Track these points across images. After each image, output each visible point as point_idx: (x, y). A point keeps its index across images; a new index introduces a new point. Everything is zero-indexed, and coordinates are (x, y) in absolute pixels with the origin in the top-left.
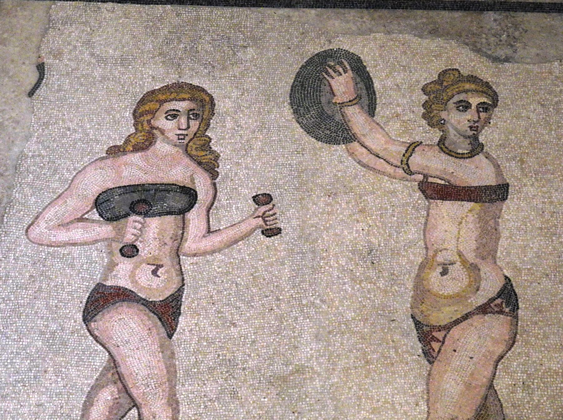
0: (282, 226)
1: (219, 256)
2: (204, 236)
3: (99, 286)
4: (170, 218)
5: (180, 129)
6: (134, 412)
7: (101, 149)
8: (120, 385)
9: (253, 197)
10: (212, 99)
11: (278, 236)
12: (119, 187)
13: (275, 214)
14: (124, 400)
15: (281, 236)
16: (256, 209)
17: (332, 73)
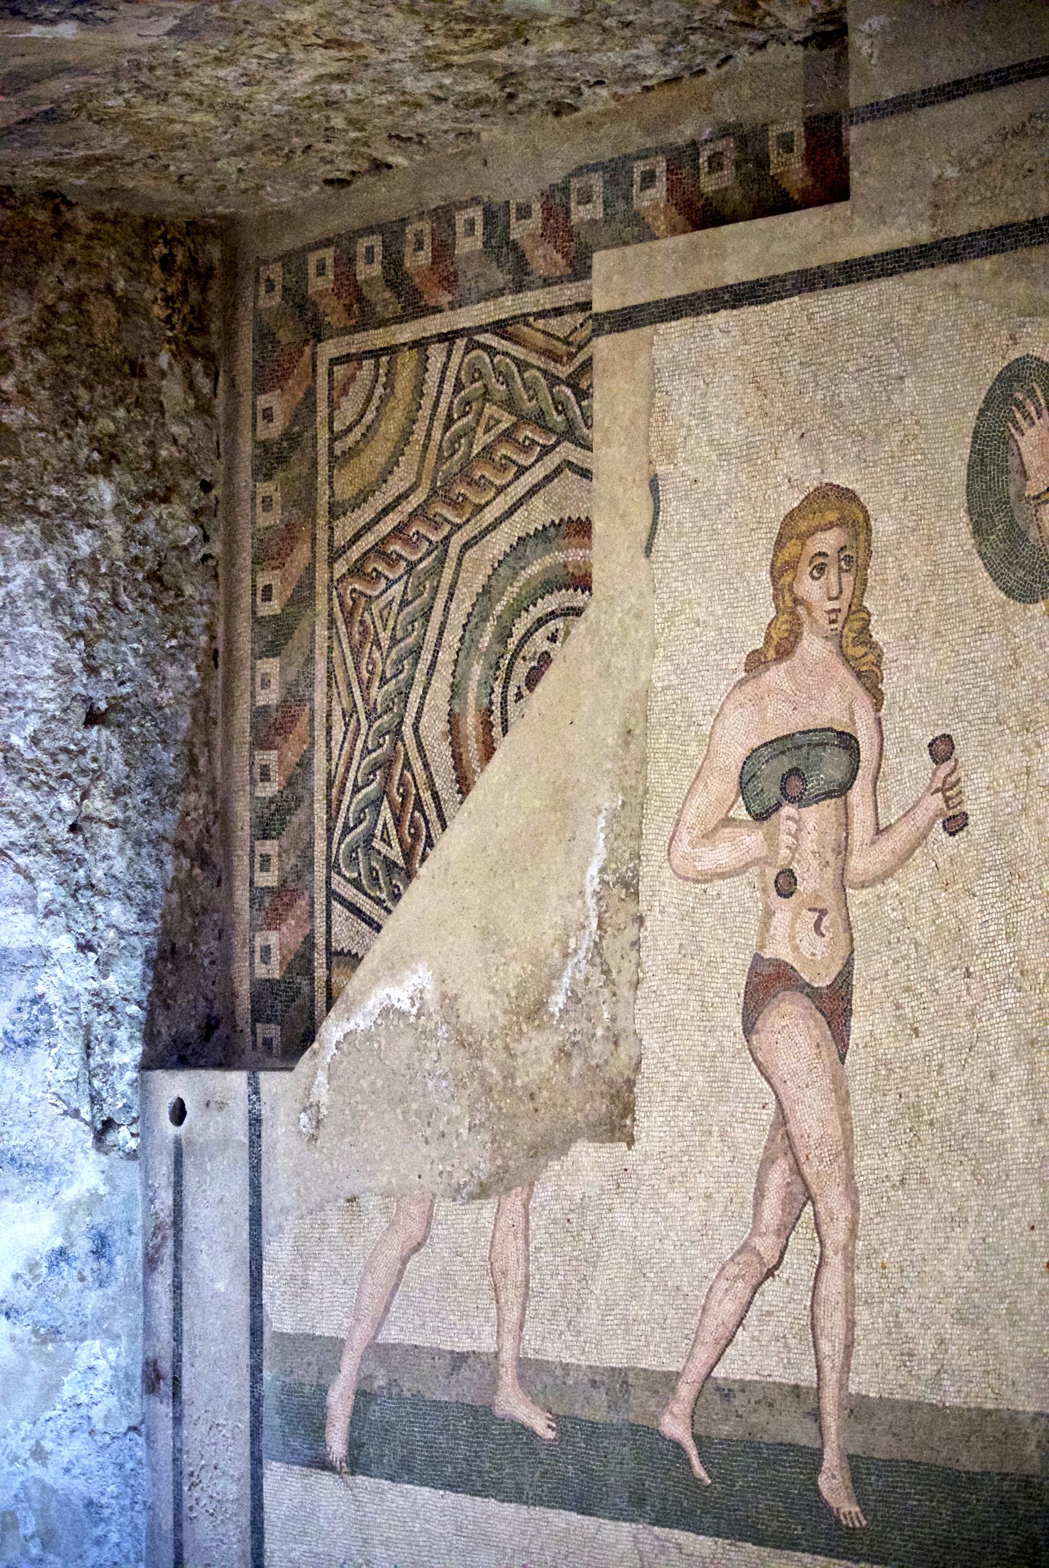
0: (967, 807)
1: (893, 886)
2: (873, 843)
3: (757, 958)
4: (829, 807)
5: (830, 599)
6: (809, 1208)
7: (737, 660)
8: (792, 1161)
9: (930, 745)
10: (867, 518)
11: (963, 834)
12: (766, 744)
13: (959, 780)
14: (797, 1188)
15: (968, 832)
16: (934, 774)
17: (1024, 424)
